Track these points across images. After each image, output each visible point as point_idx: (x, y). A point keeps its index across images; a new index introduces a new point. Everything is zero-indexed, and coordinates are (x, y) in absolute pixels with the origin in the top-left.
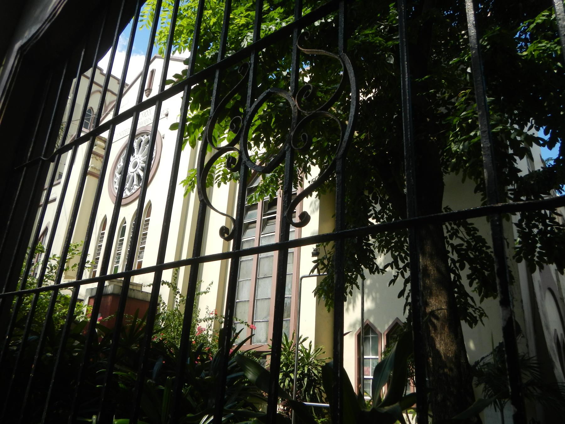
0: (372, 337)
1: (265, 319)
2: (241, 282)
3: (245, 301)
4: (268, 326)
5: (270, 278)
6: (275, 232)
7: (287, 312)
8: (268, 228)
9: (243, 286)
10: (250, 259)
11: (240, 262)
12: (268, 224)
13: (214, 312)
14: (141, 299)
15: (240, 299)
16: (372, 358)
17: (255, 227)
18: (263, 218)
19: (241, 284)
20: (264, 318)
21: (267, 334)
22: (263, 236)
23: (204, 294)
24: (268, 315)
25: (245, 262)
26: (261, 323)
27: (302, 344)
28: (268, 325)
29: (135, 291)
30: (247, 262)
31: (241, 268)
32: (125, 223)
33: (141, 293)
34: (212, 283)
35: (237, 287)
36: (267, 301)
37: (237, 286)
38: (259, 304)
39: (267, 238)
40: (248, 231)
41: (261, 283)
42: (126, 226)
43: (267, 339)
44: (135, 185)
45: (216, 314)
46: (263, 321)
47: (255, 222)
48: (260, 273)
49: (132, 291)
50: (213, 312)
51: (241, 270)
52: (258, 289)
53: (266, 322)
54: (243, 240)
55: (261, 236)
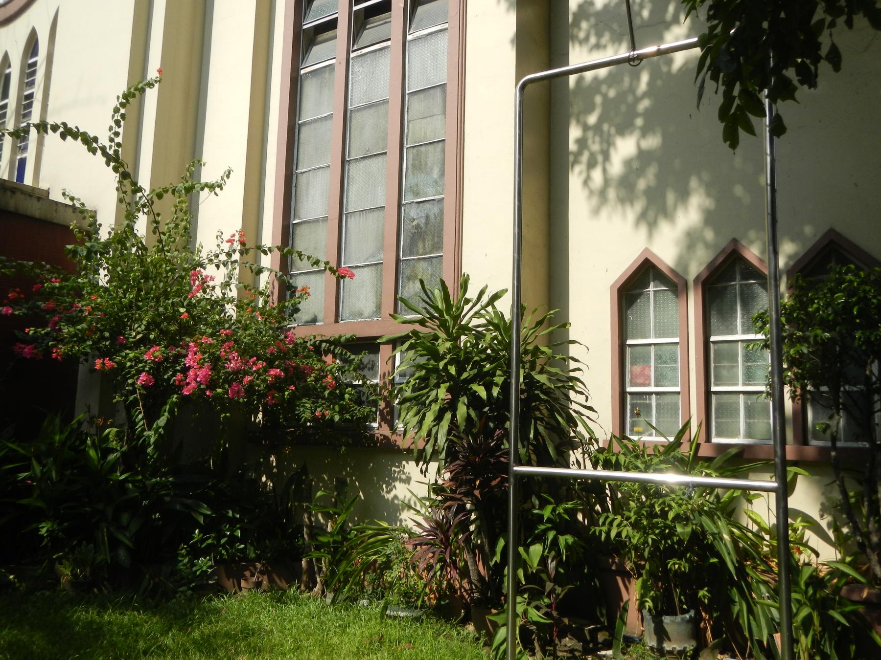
0: (655, 291)
1: (371, 259)
2: (305, 175)
3: (316, 221)
4: (380, 277)
5: (380, 159)
6: (389, 39)
7: (430, 238)
8: (368, 35)
9: (308, 183)
10: (324, 115)
11: (297, 126)
12: (368, 26)
13: (237, 238)
15: (302, 216)
16: (655, 344)
17: (335, 37)
18: (355, 8)
19: (303, 180)
20: (367, 259)
21: (379, 296)
22: (359, 53)
23: (206, 190)
24: (381, 248)
25: (312, 126)
26: (361, 270)
27: (494, 307)
28: (381, 275)
29: (18, 195)
30: (318, 125)
31: (301, 141)
32: (9, 66)
33: (35, 201)
34: (229, 173)
35: (294, 189)
36: (376, 214)
37: (294, 184)
38: (353, 225)
39: (368, 59)
40: (316, 49)
41: (355, 171)
43: (379, 307)
45: (243, 243)
46: (368, 265)
47: (332, 25)
48: (351, 147)
49: (9, 193)
50: (234, 235)
51: (300, 146)
52: (351, 187)
53: (373, 268)
54: (302, 72)
55: (352, 55)
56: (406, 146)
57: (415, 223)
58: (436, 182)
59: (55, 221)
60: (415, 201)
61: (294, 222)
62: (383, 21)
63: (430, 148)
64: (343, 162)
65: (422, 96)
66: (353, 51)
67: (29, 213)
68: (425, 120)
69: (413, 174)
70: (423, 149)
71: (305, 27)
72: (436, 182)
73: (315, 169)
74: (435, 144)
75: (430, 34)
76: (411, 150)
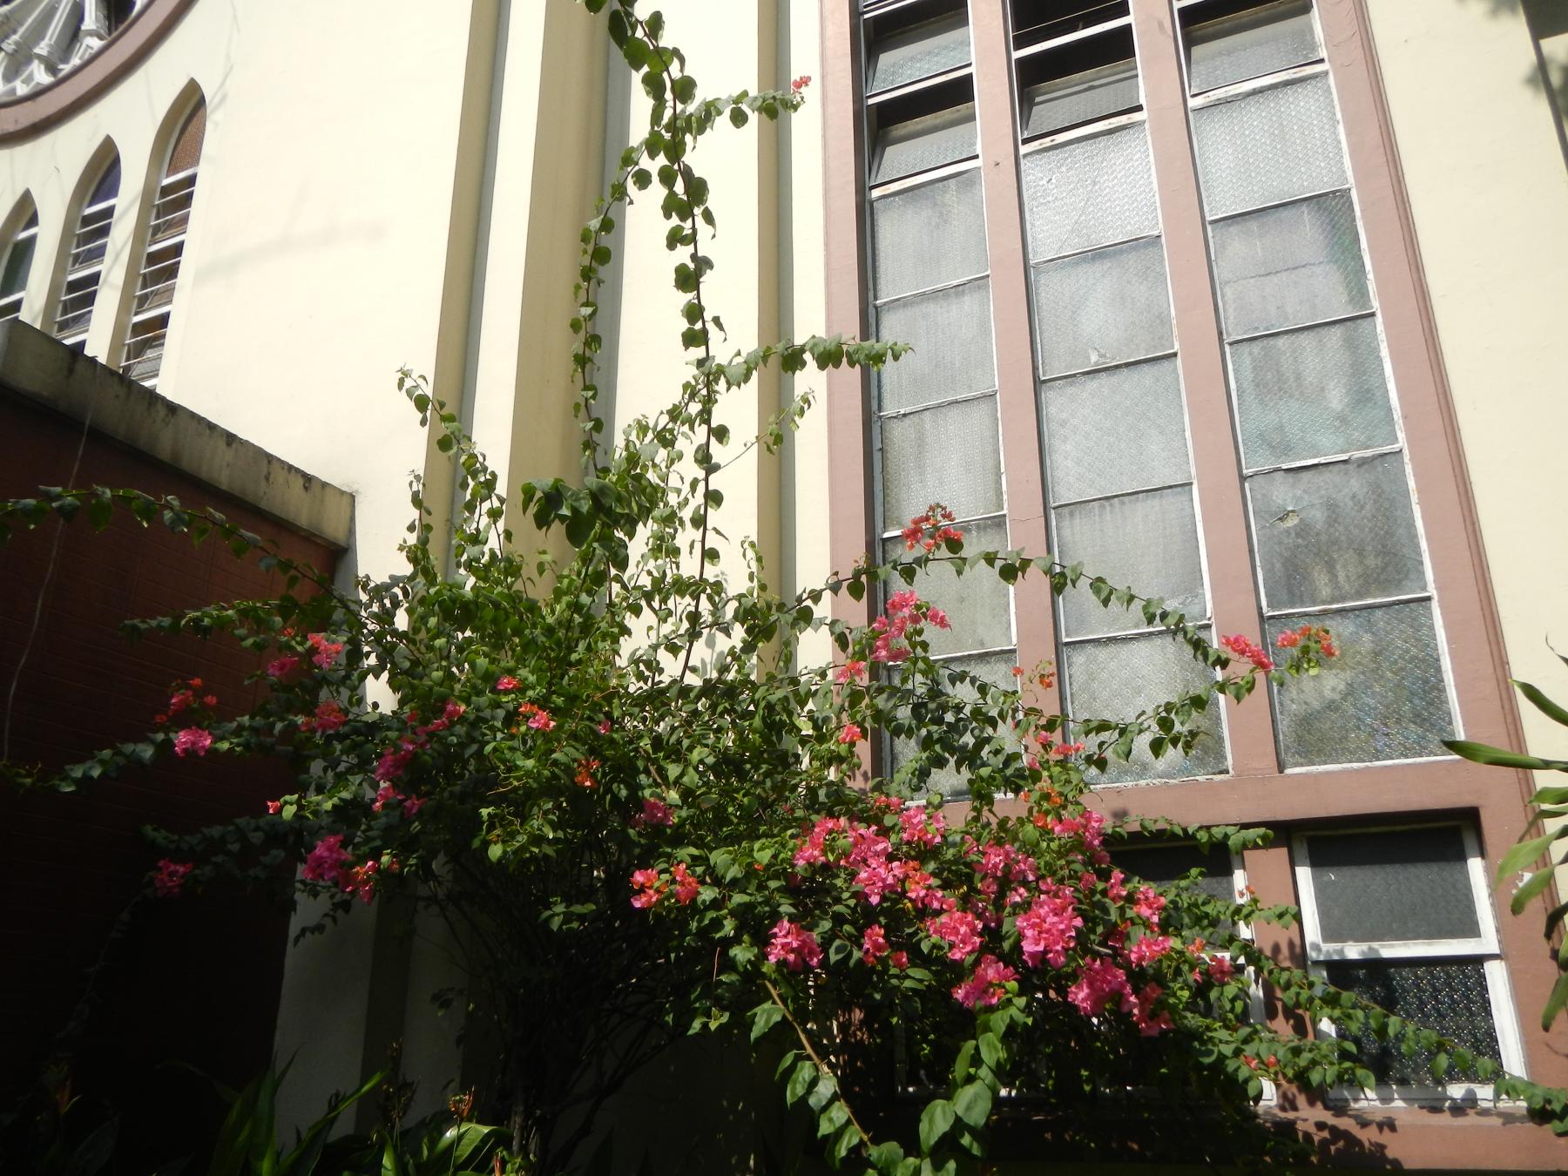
5: (1148, 373)
10: (955, 283)
12: (1038, 99)
14: (224, 487)
22: (1035, 145)
40: (891, 152)
42: (32, 240)
44: (91, 33)
56: (1227, 340)
57: (1292, 522)
58: (1343, 420)
59: (263, 505)
60: (1284, 466)
61: (886, 535)
62: (1085, 86)
63: (1305, 339)
64: (1038, 384)
65: (1253, 225)
66: (1025, 141)
67: (204, 474)
68: (1275, 279)
69: (1262, 402)
70: (1281, 342)
71: (871, 101)
72: (1343, 420)
73: (939, 406)
74: (1324, 331)
75: (1255, 92)
76: (1245, 348)
